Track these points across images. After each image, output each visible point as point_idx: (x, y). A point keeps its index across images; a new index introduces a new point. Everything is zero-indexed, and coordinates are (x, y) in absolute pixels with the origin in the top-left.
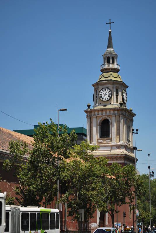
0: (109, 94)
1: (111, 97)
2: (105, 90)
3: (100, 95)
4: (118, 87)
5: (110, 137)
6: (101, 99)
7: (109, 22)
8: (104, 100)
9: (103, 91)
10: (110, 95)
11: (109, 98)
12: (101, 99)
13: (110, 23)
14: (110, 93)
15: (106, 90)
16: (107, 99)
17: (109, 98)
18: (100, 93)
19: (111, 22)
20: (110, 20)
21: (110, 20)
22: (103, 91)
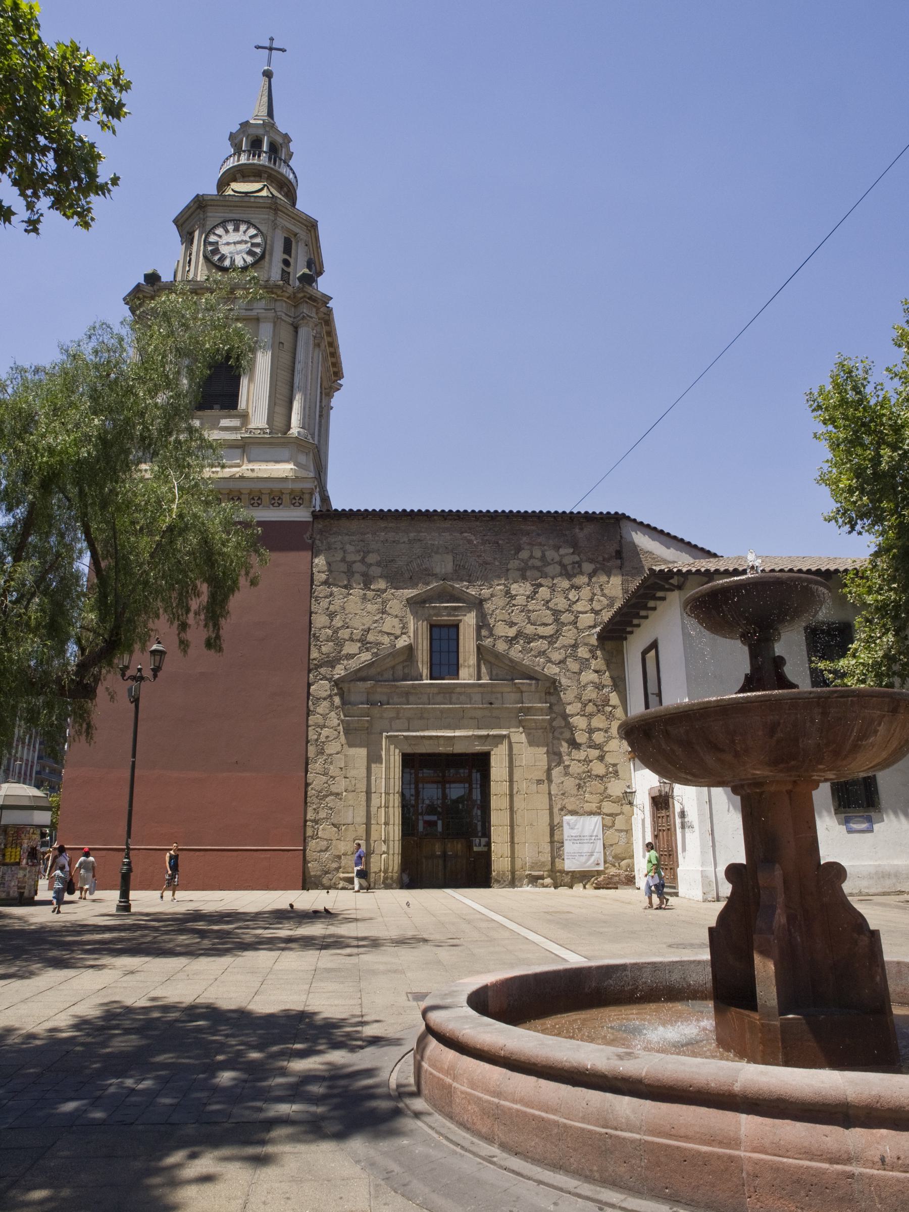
0: (253, 245)
1: (263, 256)
2: (236, 229)
3: (211, 244)
4: (295, 235)
5: (242, 405)
6: (216, 258)
7: (267, 44)
8: (227, 263)
9: (227, 231)
10: (258, 250)
11: (249, 259)
12: (216, 258)
13: (271, 49)
14: (258, 240)
15: (243, 227)
16: (239, 263)
17: (249, 259)
18: (213, 238)
19: (274, 46)
20: (272, 39)
21: (272, 39)
22: (227, 231)
